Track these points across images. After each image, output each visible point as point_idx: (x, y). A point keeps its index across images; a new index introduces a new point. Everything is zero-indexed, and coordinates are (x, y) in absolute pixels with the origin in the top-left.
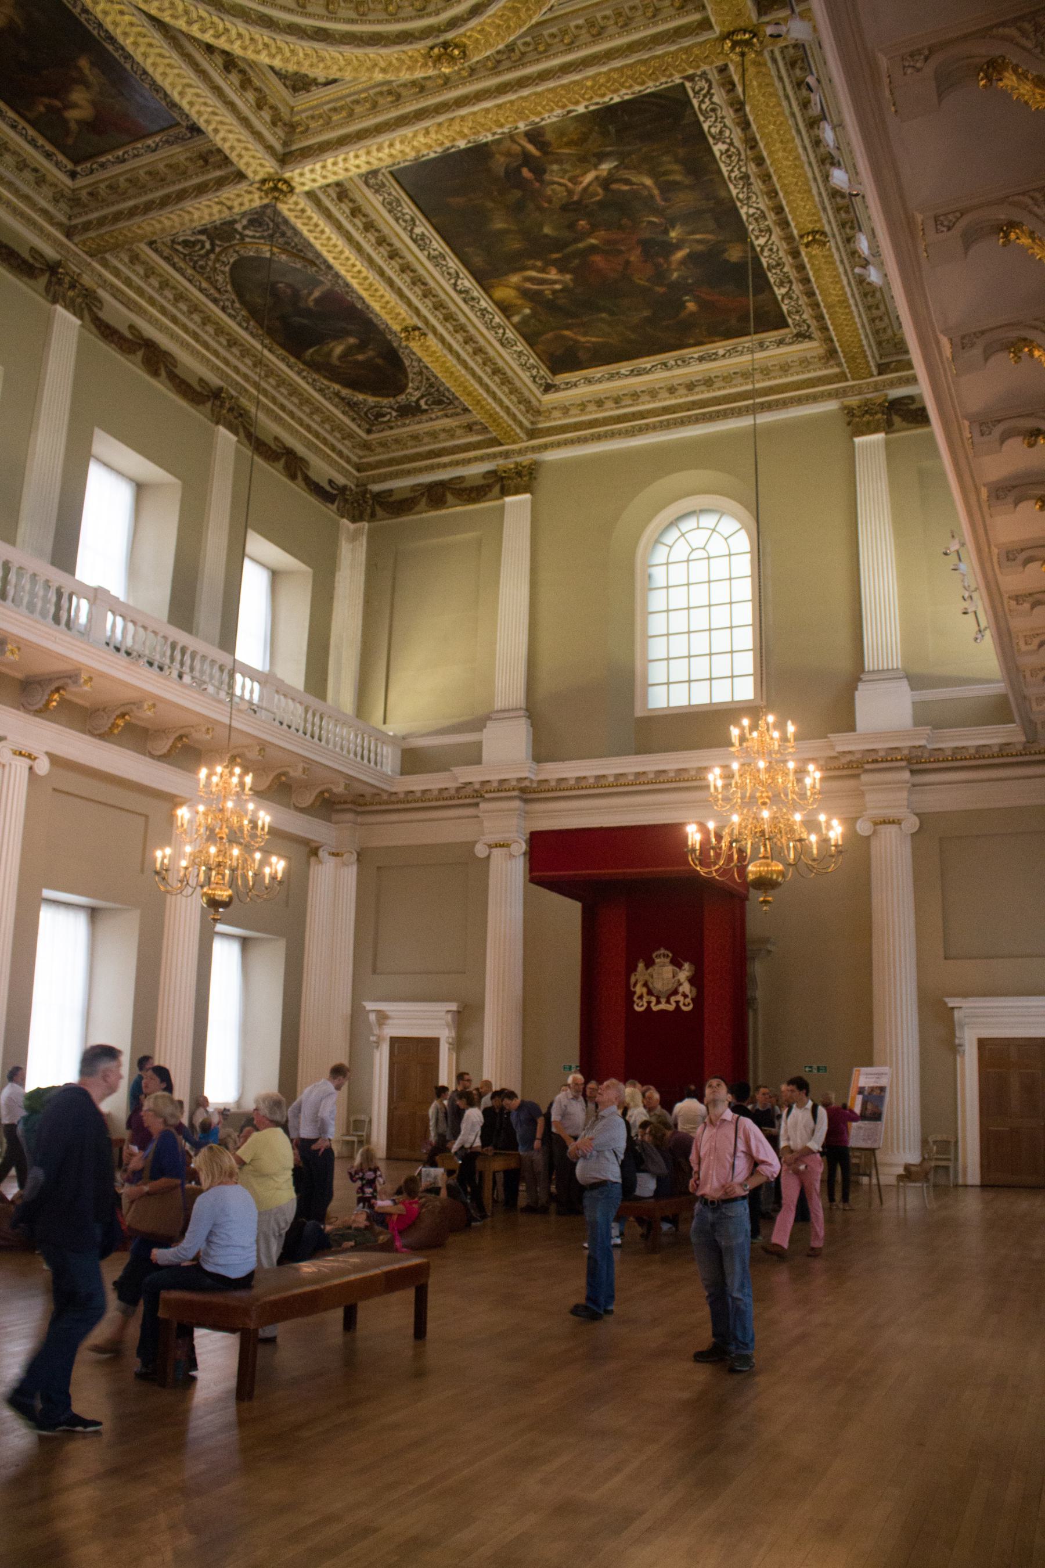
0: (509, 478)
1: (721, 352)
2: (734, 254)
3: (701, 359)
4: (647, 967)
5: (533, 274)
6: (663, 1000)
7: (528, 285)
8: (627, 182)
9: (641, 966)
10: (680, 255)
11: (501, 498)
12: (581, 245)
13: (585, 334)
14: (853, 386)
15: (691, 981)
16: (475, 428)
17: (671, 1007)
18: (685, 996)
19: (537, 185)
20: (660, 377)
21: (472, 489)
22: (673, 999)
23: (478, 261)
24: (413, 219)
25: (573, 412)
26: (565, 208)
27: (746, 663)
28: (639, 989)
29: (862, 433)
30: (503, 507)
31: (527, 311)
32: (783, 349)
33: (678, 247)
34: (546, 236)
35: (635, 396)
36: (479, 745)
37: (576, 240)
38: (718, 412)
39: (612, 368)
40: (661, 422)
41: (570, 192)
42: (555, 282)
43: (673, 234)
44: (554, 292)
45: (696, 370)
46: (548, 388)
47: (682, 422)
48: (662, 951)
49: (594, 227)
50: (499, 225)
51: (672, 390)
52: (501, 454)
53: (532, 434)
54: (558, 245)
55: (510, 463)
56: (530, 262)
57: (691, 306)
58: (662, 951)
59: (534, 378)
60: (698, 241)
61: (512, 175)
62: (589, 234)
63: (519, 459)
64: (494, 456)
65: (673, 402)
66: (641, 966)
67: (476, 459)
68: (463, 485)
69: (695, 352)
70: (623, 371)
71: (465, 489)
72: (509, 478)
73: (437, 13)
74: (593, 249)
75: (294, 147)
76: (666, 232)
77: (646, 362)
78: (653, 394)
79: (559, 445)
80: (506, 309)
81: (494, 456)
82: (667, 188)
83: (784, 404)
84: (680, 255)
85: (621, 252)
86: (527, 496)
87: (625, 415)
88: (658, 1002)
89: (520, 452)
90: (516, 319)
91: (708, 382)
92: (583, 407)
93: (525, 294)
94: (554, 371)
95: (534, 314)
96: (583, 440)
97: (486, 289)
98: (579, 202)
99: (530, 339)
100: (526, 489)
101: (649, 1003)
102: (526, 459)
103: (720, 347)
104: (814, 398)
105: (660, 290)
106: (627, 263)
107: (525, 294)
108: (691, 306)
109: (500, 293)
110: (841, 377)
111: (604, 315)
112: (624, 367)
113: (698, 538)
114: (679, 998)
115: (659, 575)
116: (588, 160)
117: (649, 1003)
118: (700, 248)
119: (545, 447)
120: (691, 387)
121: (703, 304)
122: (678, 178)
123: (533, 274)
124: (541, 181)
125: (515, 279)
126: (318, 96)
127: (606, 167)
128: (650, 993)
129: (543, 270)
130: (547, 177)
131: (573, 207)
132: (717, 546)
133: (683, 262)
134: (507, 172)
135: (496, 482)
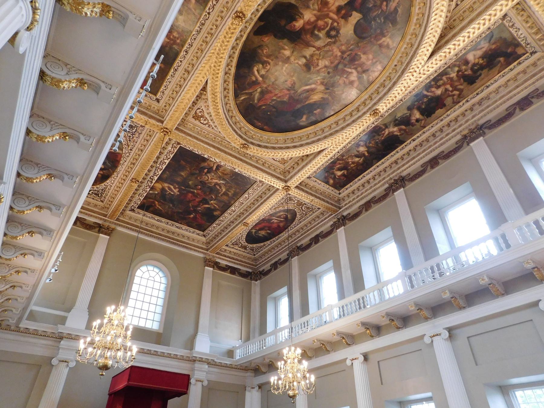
1: (184, 228)
2: (216, 213)
3: (177, 227)
5: (172, 187)
7: (167, 189)
8: (220, 187)
12: (192, 190)
14: (208, 253)
16: (98, 206)
20: (163, 225)
21: (88, 225)
23: (165, 176)
26: (201, 182)
27: (158, 317)
29: (208, 267)
30: (99, 236)
32: (197, 236)
33: (209, 204)
37: (192, 189)
38: (173, 242)
39: (154, 216)
40: (157, 237)
41: (207, 180)
42: (173, 192)
43: (212, 202)
44: (170, 193)
45: (174, 229)
46: (133, 210)
47: (163, 240)
50: (183, 174)
51: (163, 230)
52: (104, 219)
53: (118, 220)
54: (188, 186)
55: (107, 224)
57: (192, 216)
59: (133, 206)
60: (214, 206)
61: (204, 168)
62: (197, 189)
63: (110, 225)
64: (101, 219)
65: (162, 233)
67: (94, 217)
68: (85, 222)
69: (178, 225)
70: (156, 219)
71: (85, 224)
72: (104, 228)
73: (249, 138)
74: (193, 193)
75: (180, 128)
77: (164, 220)
78: (157, 228)
79: (124, 227)
81: (101, 219)
82: (225, 194)
83: (191, 249)
87: (147, 229)
89: (110, 222)
90: (151, 192)
91: (173, 233)
93: (163, 189)
94: (139, 208)
95: (156, 194)
97: (157, 181)
98: (206, 183)
99: (146, 197)
100: (109, 235)
102: (113, 226)
103: (184, 227)
104: (199, 251)
105: (192, 209)
106: (195, 200)
107: (163, 189)
108: (192, 216)
110: (207, 250)
112: (157, 218)
113: (153, 274)
115: (136, 280)
116: (220, 178)
118: (213, 207)
119: (120, 225)
120: (168, 232)
121: (195, 218)
122: (230, 194)
123: (172, 187)
125: (166, 185)
126: (197, 122)
127: (221, 182)
129: (175, 188)
130: (208, 175)
131: (203, 183)
132: (157, 278)
133: (205, 208)
134: (202, 167)
135: (98, 227)
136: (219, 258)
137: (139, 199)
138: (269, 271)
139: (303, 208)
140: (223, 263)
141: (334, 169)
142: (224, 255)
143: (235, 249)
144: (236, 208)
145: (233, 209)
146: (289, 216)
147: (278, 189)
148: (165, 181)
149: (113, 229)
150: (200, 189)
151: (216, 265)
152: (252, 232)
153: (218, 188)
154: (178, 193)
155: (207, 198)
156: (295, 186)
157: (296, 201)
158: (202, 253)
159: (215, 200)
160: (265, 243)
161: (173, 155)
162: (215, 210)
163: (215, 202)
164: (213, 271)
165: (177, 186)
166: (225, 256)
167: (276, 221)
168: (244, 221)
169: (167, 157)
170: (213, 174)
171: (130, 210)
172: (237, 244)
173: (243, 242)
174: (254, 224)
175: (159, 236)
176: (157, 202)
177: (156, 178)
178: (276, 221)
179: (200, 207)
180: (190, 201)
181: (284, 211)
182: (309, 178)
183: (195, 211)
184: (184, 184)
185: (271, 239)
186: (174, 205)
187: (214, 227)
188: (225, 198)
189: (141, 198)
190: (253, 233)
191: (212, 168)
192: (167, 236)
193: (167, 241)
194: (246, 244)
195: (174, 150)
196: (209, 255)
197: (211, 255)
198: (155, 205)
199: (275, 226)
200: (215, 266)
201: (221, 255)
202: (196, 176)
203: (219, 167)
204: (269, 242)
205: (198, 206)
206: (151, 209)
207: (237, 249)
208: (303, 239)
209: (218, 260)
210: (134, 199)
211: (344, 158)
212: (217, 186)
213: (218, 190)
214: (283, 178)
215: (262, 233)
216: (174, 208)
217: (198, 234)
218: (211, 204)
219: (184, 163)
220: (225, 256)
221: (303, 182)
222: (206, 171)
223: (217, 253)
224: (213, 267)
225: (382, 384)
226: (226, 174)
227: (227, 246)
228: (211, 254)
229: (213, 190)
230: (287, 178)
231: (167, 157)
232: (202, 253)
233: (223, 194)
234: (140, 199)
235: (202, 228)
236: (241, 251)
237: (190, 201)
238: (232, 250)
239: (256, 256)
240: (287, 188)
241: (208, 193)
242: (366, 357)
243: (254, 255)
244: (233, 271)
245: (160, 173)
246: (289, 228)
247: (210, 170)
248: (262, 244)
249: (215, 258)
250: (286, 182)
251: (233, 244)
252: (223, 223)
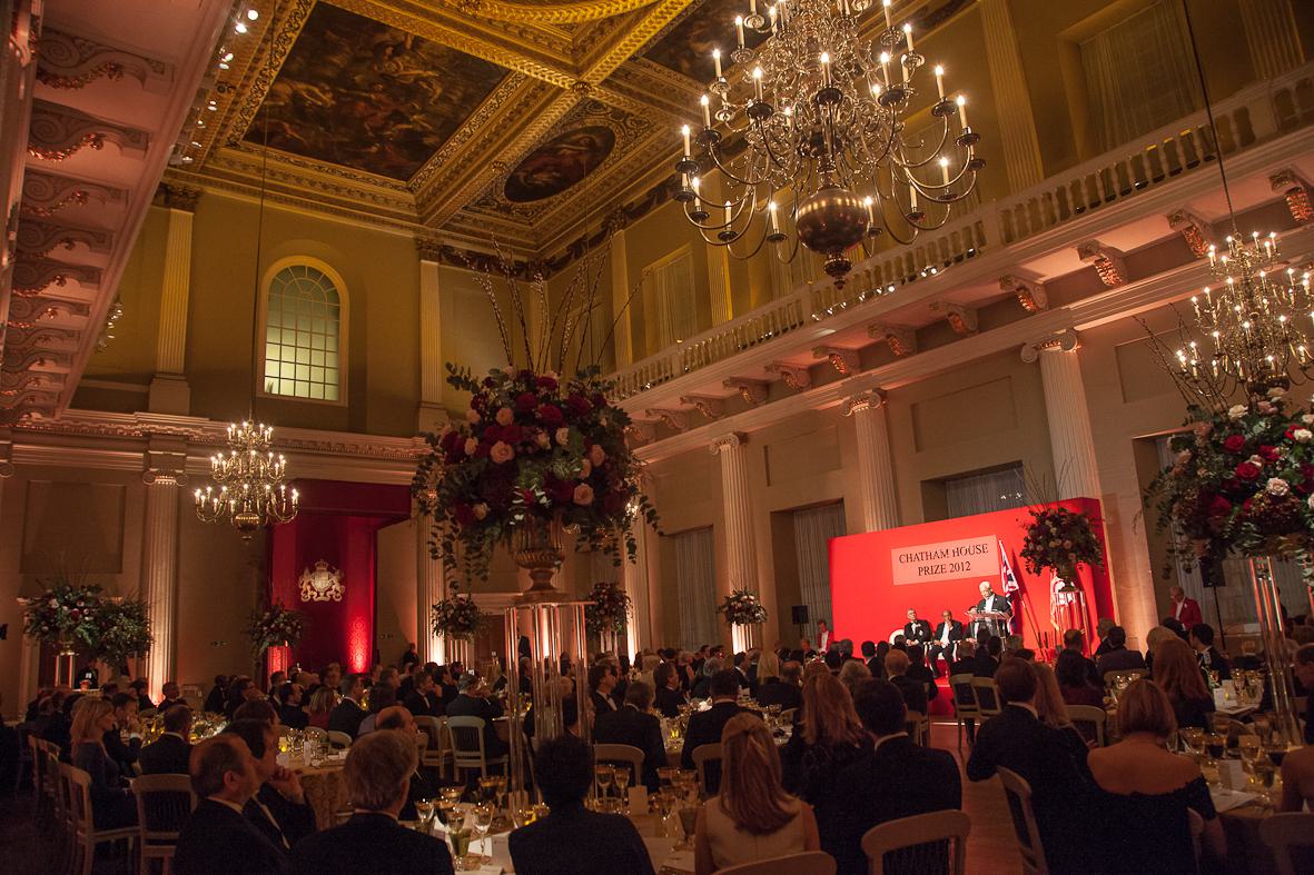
0: (176, 194)
2: (428, 141)
4: (311, 572)
5: (316, 90)
6: (322, 594)
7: (304, 94)
8: (430, 85)
9: (307, 571)
10: (405, 126)
11: (169, 207)
12: (364, 94)
13: (296, 132)
15: (341, 582)
17: (327, 599)
18: (337, 592)
19: (386, 58)
22: (328, 593)
23: (294, 67)
24: (297, 29)
25: (251, 170)
26: (382, 75)
27: (331, 376)
28: (305, 587)
31: (282, 103)
33: (409, 123)
34: (353, 80)
35: (286, 176)
36: (147, 395)
42: (321, 100)
43: (415, 117)
45: (337, 179)
46: (233, 145)
47: (316, 208)
48: (322, 562)
49: (383, 91)
51: (312, 183)
54: (355, 86)
56: (322, 84)
57: (374, 149)
58: (322, 562)
59: (232, 136)
60: (422, 126)
61: (383, 46)
62: (374, 92)
66: (307, 571)
70: (292, 160)
74: (367, 100)
76: (413, 114)
77: (311, 161)
78: (299, 180)
79: (222, 186)
80: (272, 95)
82: (443, 98)
83: (383, 222)
84: (405, 126)
85: (379, 108)
86: (192, 214)
87: (275, 186)
88: (318, 595)
89: (188, 178)
91: (338, 189)
92: (245, 167)
93: (296, 96)
94: (247, 138)
95: (281, 107)
96: (239, 190)
97: (278, 80)
98: (393, 78)
99: (260, 116)
100: (191, 209)
101: (312, 596)
102: (195, 186)
103: (362, 173)
104: (402, 227)
105: (370, 134)
106: (375, 114)
107: (296, 96)
109: (285, 89)
110: (421, 221)
111: (322, 129)
112: (294, 157)
114: (331, 592)
116: (425, 65)
117: (312, 596)
118: (419, 129)
119: (211, 183)
120: (325, 187)
121: (382, 152)
122: (453, 98)
123: (316, 90)
124: (390, 58)
125: (301, 86)
127: (430, 73)
128: (312, 589)
129: (324, 92)
130: (396, 59)
131: (387, 79)
133: (401, 130)
136: (449, 237)
137: (242, 122)
138: (565, 261)
139: (628, 123)
140: (461, 247)
141: (687, 39)
142: (461, 229)
143: (485, 213)
144: (473, 128)
145: (468, 130)
146: (598, 140)
147: (562, 90)
148: (298, 77)
149: (198, 194)
150: (383, 91)
151: (446, 254)
152: (518, 177)
153: (425, 87)
154: (334, 102)
155: (403, 109)
156: (601, 79)
157: (610, 110)
158: (410, 228)
159: (421, 113)
160: (552, 198)
161: (305, 20)
162: (425, 133)
163: (420, 117)
164: (439, 268)
165: (327, 88)
166: (464, 231)
167: (569, 152)
168: (496, 158)
169: (291, 26)
170: (407, 58)
171: (227, 146)
172: (487, 204)
173: (501, 198)
174: (520, 161)
175: (306, 200)
176: (286, 125)
177: (275, 74)
178: (569, 152)
179: (387, 130)
180: (363, 119)
181: (586, 130)
182: (632, 59)
183: (380, 139)
184: (341, 81)
185: (564, 189)
186: (328, 129)
187: (430, 171)
188: (444, 108)
189: (247, 118)
190: (522, 179)
191: (402, 44)
192: (325, 198)
193: (327, 210)
194: (509, 202)
195: (304, 10)
196: (427, 233)
197: (430, 232)
198: (285, 131)
199: (568, 162)
200: (443, 257)
201: (454, 230)
202: (368, 63)
203: (418, 41)
204: (559, 196)
205: (383, 128)
206: (278, 139)
207: (489, 214)
208: (633, 190)
209: (448, 242)
210: (233, 123)
211: (710, 14)
212: (421, 83)
213: (426, 91)
214: (571, 63)
215: (542, 178)
216: (330, 135)
217: (395, 187)
218: (414, 121)
219: (334, 36)
220: (464, 231)
221: (618, 69)
222: (389, 51)
223: (445, 227)
224: (440, 260)
225: (769, 485)
226: (438, 57)
227: (466, 208)
228: (429, 229)
229: (413, 90)
230: (581, 64)
231: (291, 26)
232: (410, 228)
233: (439, 98)
234: (247, 121)
235: (401, 173)
236: (500, 219)
237: (363, 119)
238: (478, 216)
239: (534, 227)
240: (583, 87)
241: (402, 99)
242: (743, 438)
243: (531, 224)
244: (482, 262)
245: (282, 61)
246: (602, 165)
247: (399, 49)
248: (545, 201)
249: (442, 239)
250: (578, 71)
251: (478, 204)
252: (447, 162)
